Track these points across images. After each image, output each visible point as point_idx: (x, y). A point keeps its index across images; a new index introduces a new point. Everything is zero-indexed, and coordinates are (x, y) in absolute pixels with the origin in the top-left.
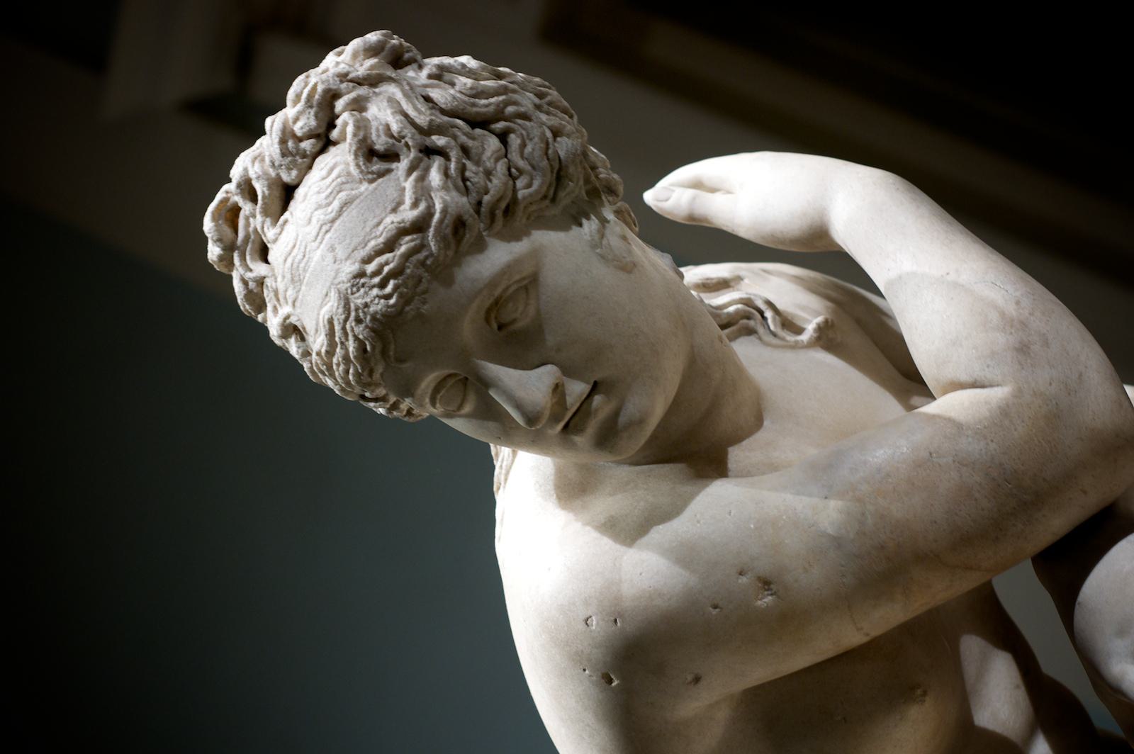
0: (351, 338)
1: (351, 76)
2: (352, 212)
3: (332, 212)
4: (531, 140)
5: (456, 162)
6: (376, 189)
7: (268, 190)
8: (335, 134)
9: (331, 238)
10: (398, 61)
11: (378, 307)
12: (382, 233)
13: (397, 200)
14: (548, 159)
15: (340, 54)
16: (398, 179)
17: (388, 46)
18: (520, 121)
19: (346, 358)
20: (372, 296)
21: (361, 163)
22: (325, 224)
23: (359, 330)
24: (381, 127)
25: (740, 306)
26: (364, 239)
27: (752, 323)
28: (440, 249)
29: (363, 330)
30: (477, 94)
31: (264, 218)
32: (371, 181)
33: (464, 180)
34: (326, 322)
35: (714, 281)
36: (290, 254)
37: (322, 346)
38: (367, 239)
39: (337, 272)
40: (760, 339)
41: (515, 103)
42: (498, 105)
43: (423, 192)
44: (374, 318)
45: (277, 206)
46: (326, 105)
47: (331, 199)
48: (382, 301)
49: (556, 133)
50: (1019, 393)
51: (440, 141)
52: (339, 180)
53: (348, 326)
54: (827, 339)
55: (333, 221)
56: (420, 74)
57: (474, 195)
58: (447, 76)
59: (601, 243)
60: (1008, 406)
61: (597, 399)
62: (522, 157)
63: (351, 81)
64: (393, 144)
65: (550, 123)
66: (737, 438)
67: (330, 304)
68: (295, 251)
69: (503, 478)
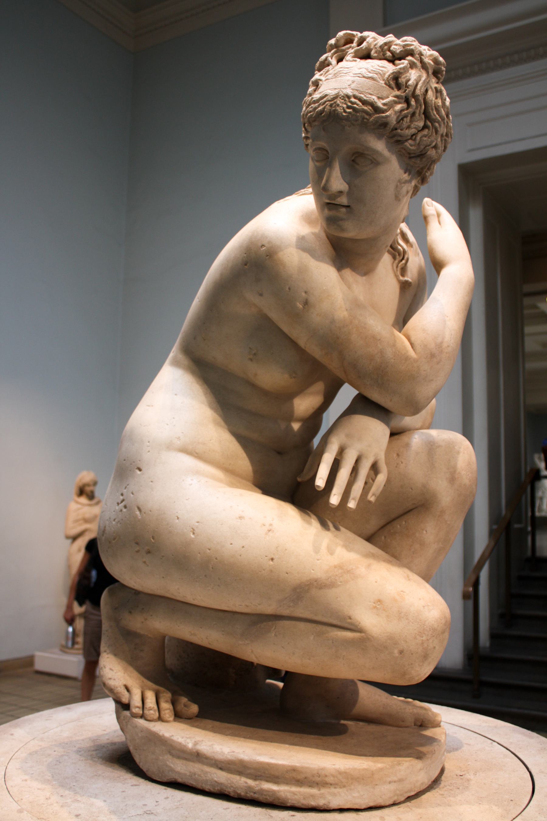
0: (324, 106)
1: (423, 57)
2: (371, 82)
3: (367, 75)
4: (429, 138)
5: (408, 112)
6: (383, 87)
7: (365, 48)
8: (397, 62)
9: (357, 79)
10: (436, 73)
11: (340, 110)
12: (368, 97)
13: (383, 97)
14: (424, 148)
15: (429, 50)
16: (391, 94)
17: (440, 66)
18: (434, 130)
19: (315, 108)
20: (343, 106)
21: (391, 77)
22: (362, 75)
23: (328, 107)
24: (408, 77)
25: (402, 250)
26: (362, 92)
27: (398, 257)
28: (372, 122)
29: (328, 109)
30: (437, 109)
31: (353, 52)
32: (385, 84)
33: (402, 119)
34: (325, 94)
35: (407, 237)
36: (344, 68)
37: (316, 98)
38: (363, 93)
39: (346, 88)
40: (393, 262)
41: (440, 125)
42: (436, 119)
43: (390, 105)
44: (335, 111)
45: (361, 55)
46: (408, 53)
47: (372, 72)
48: (342, 110)
49: (435, 147)
50: (416, 361)
51: (413, 102)
52: (381, 71)
53: (327, 103)
54: (404, 286)
55: (364, 77)
56: (435, 84)
57: (398, 126)
58: (439, 95)
59: (402, 184)
60: (410, 359)
61: (344, 210)
62: (421, 137)
63: (421, 58)
64: (404, 85)
65: (438, 143)
66: (354, 269)
67: (332, 92)
68: (347, 69)
69: (301, 193)
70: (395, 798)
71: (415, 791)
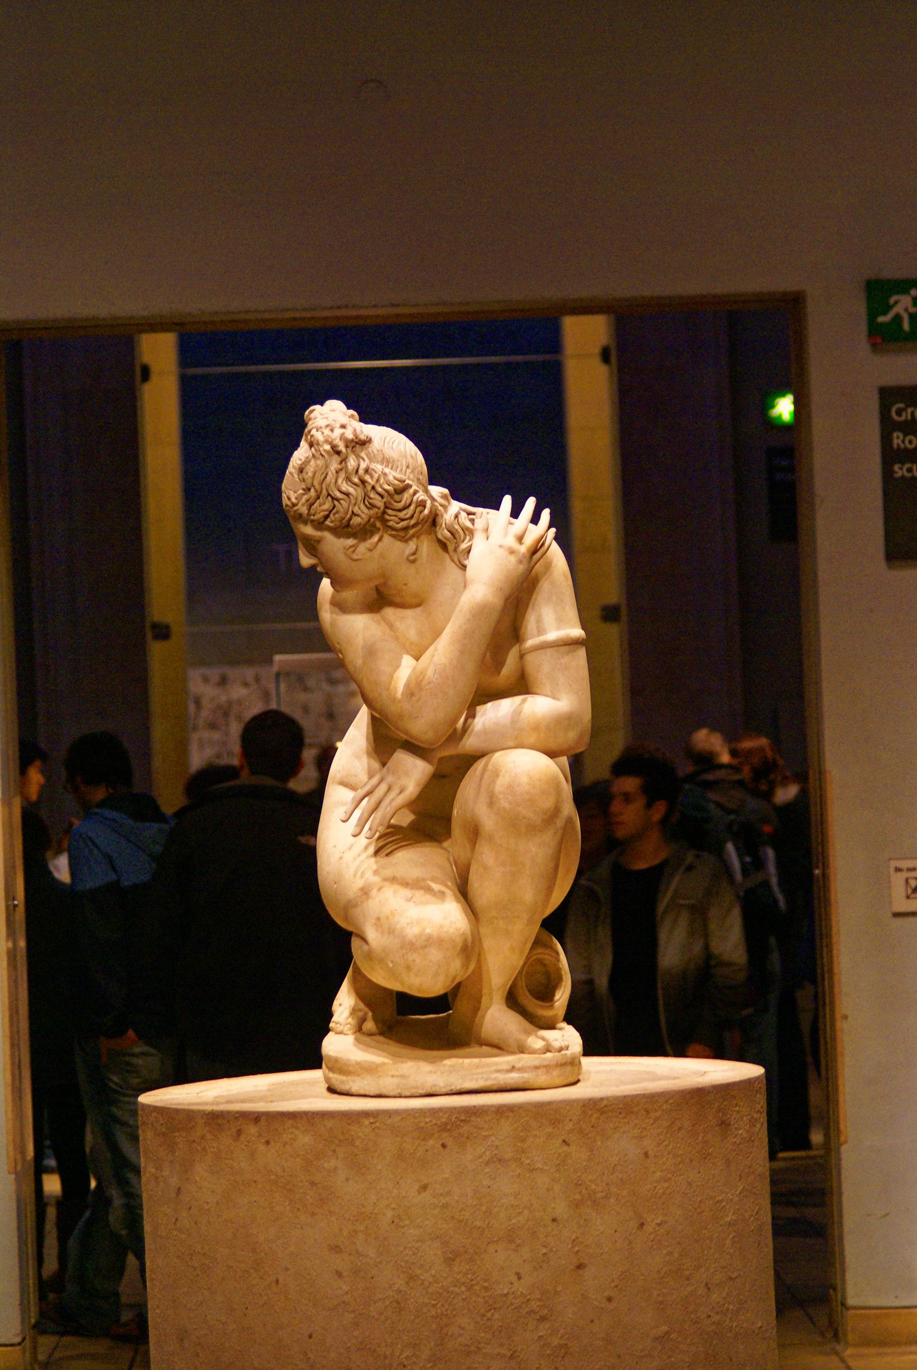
50: (400, 702)
70: (399, 1091)
71: (423, 1089)
